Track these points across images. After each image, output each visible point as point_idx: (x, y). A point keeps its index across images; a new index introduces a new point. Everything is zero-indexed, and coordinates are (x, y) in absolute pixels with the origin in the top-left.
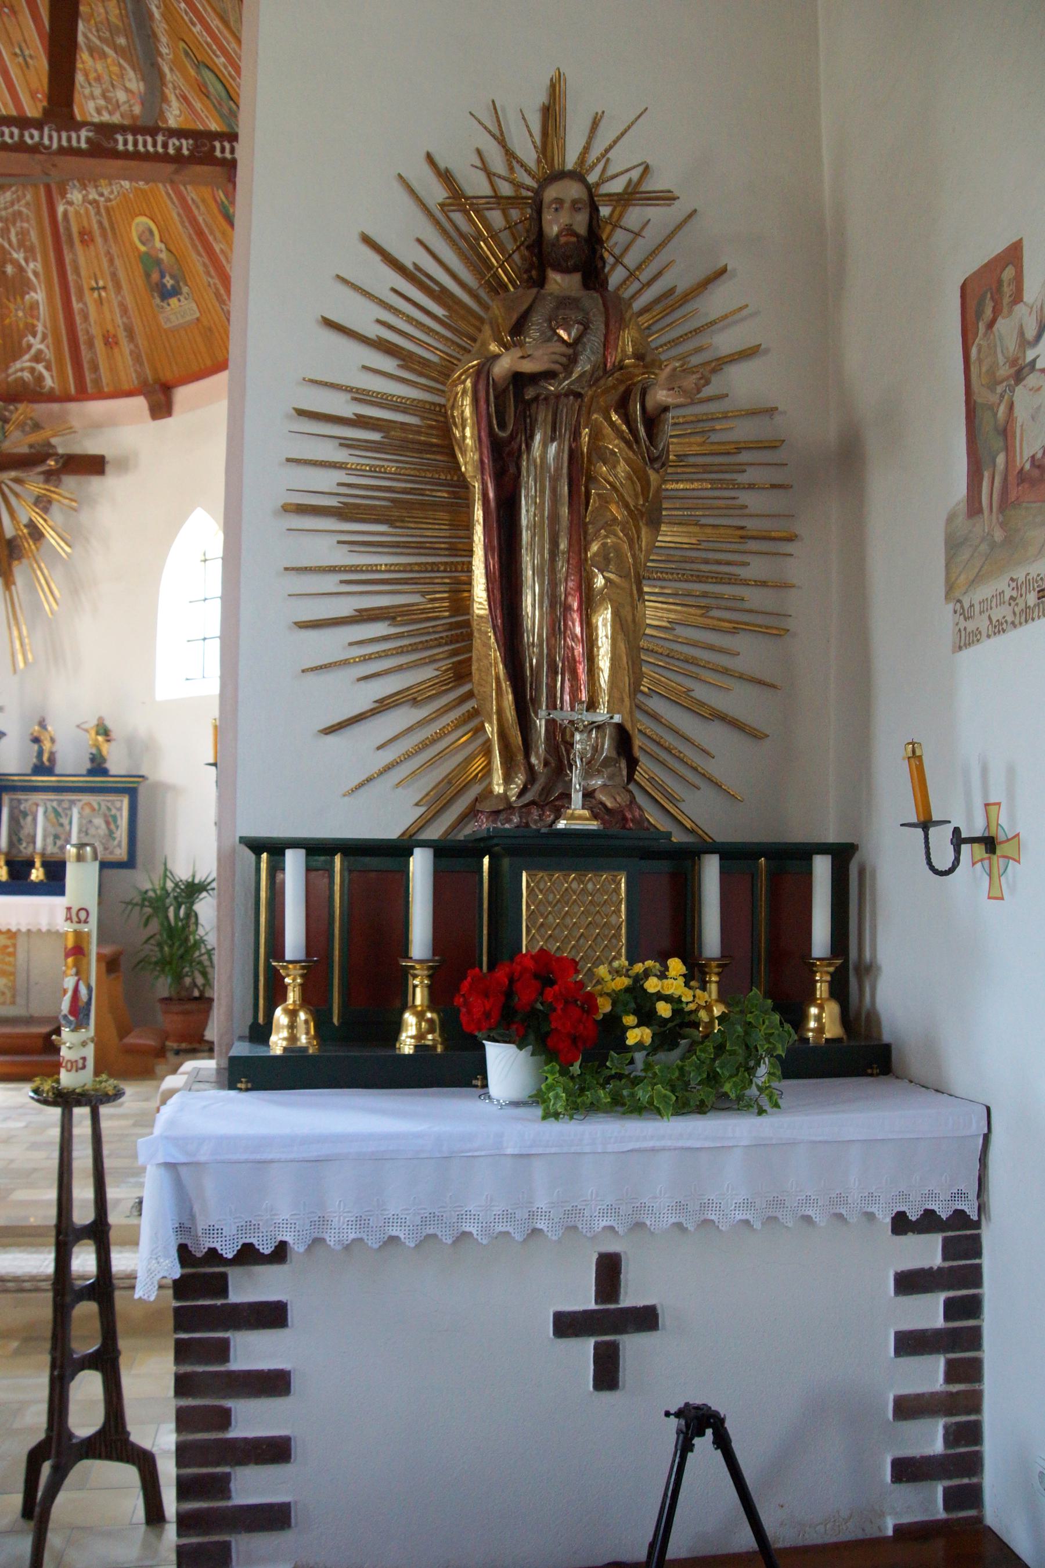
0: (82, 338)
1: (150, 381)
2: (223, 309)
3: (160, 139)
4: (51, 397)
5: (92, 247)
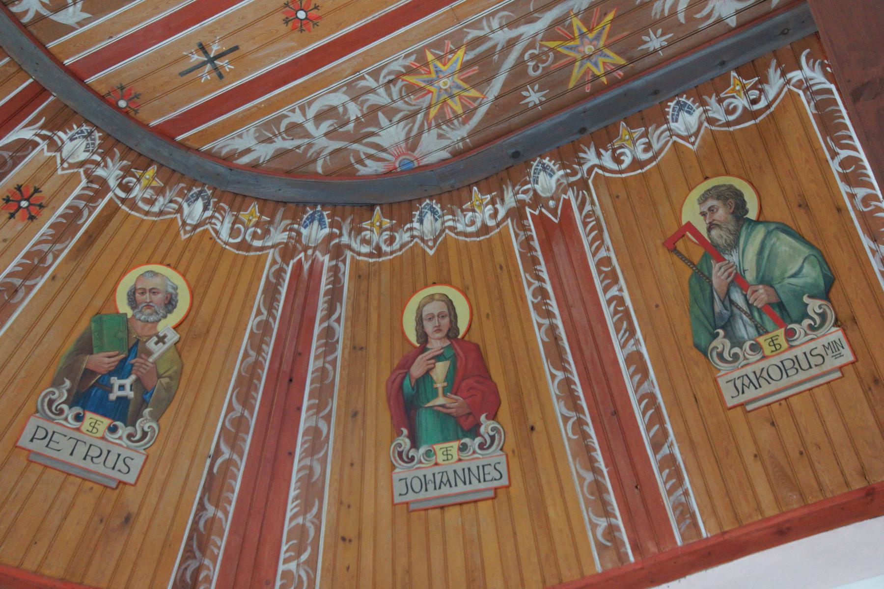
2: (201, 507)
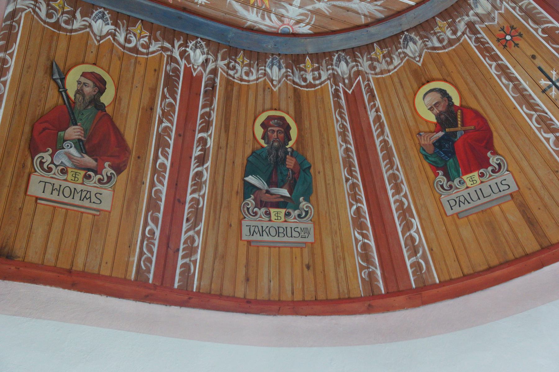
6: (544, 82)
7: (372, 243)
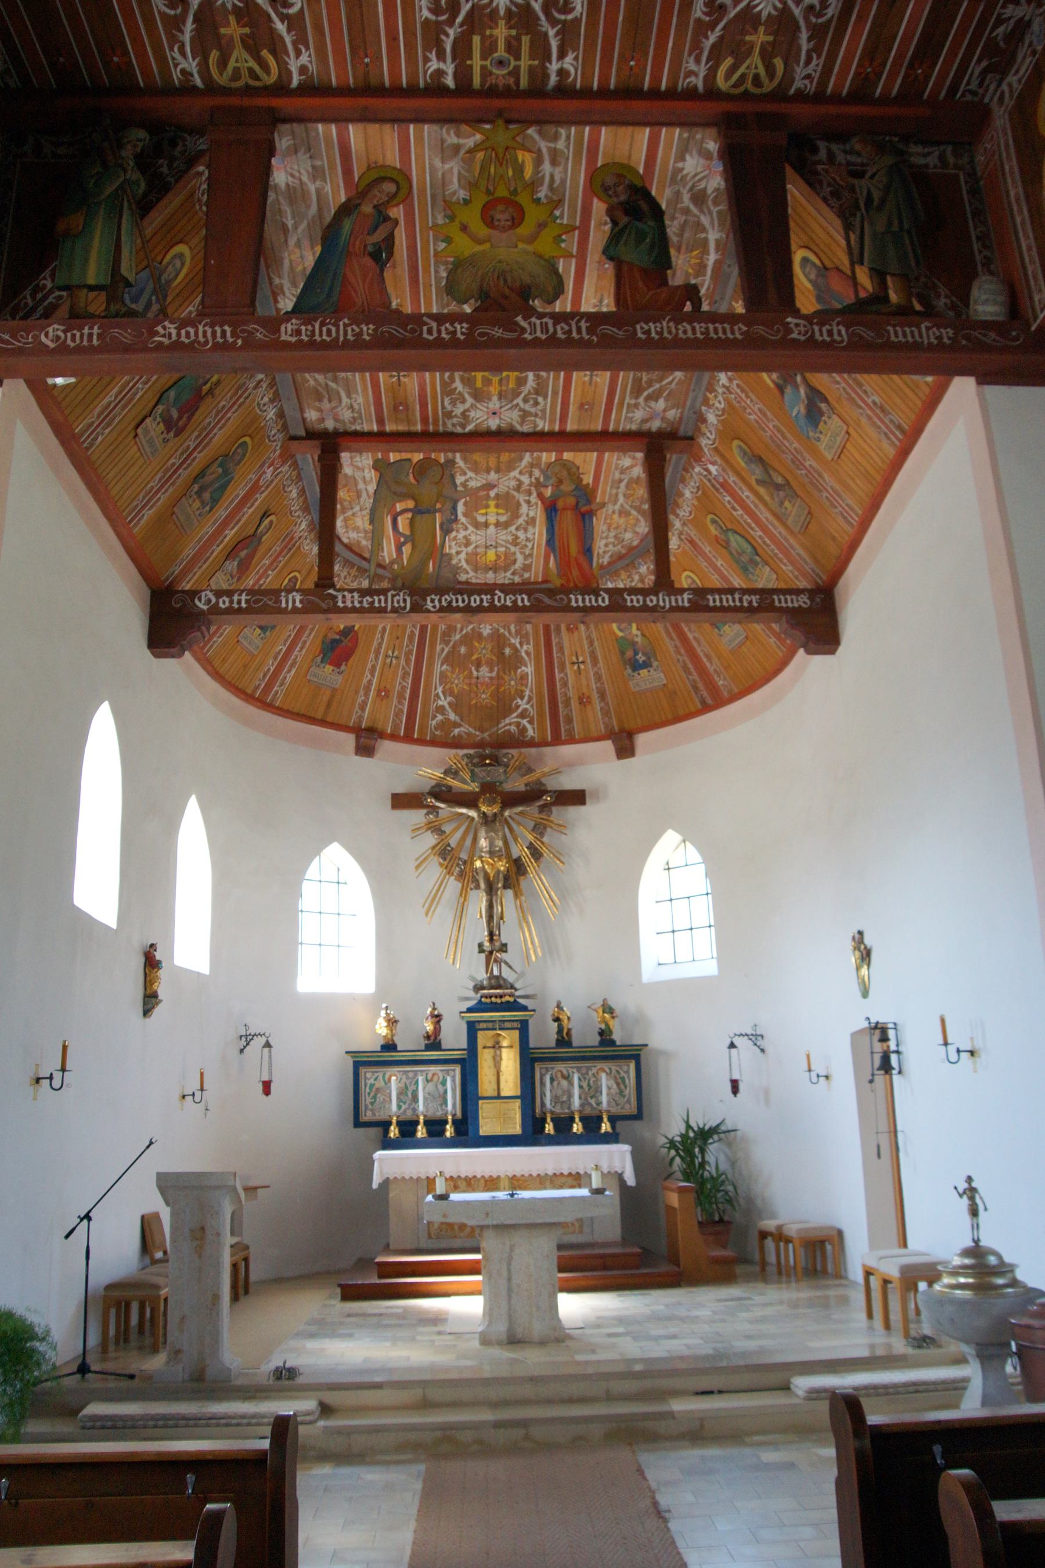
0: (560, 699)
1: (616, 729)
3: (737, 596)
4: (531, 744)
5: (576, 634)
6: (390, 653)
7: (272, 669)
